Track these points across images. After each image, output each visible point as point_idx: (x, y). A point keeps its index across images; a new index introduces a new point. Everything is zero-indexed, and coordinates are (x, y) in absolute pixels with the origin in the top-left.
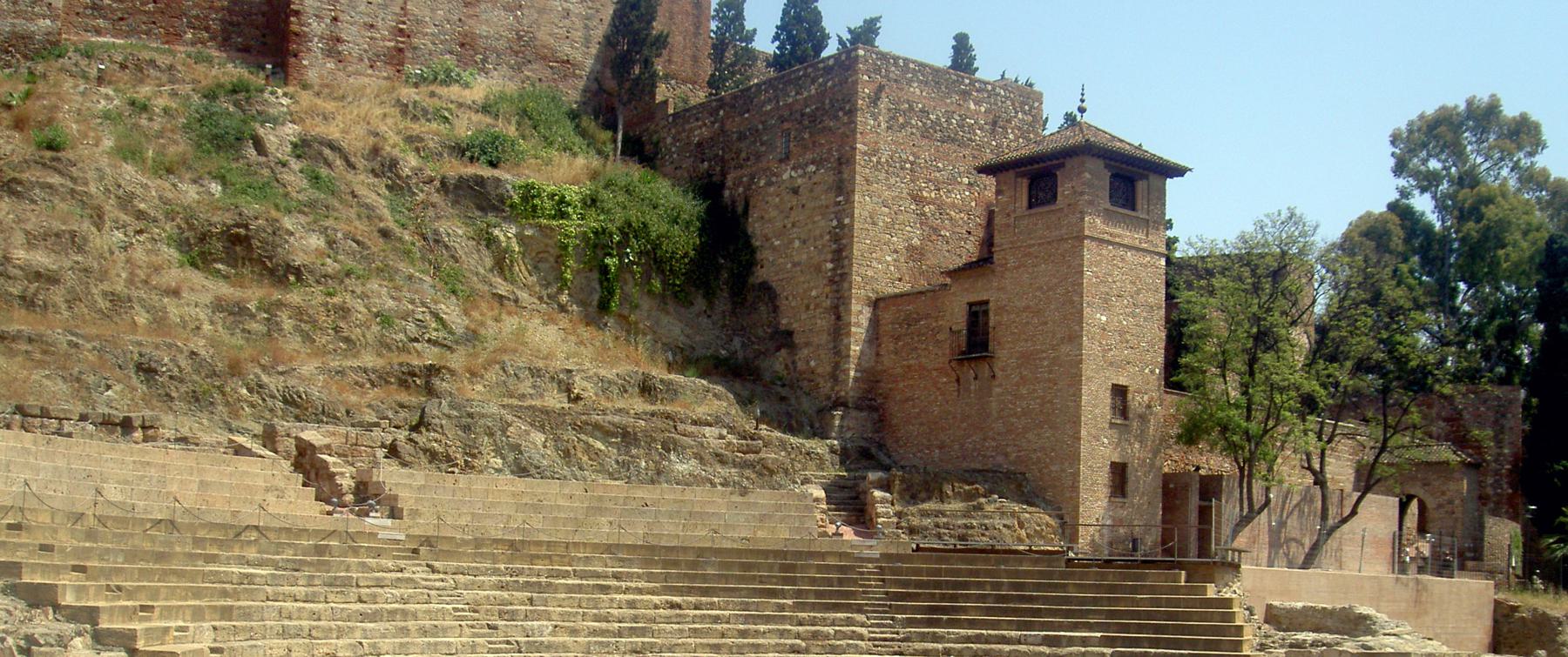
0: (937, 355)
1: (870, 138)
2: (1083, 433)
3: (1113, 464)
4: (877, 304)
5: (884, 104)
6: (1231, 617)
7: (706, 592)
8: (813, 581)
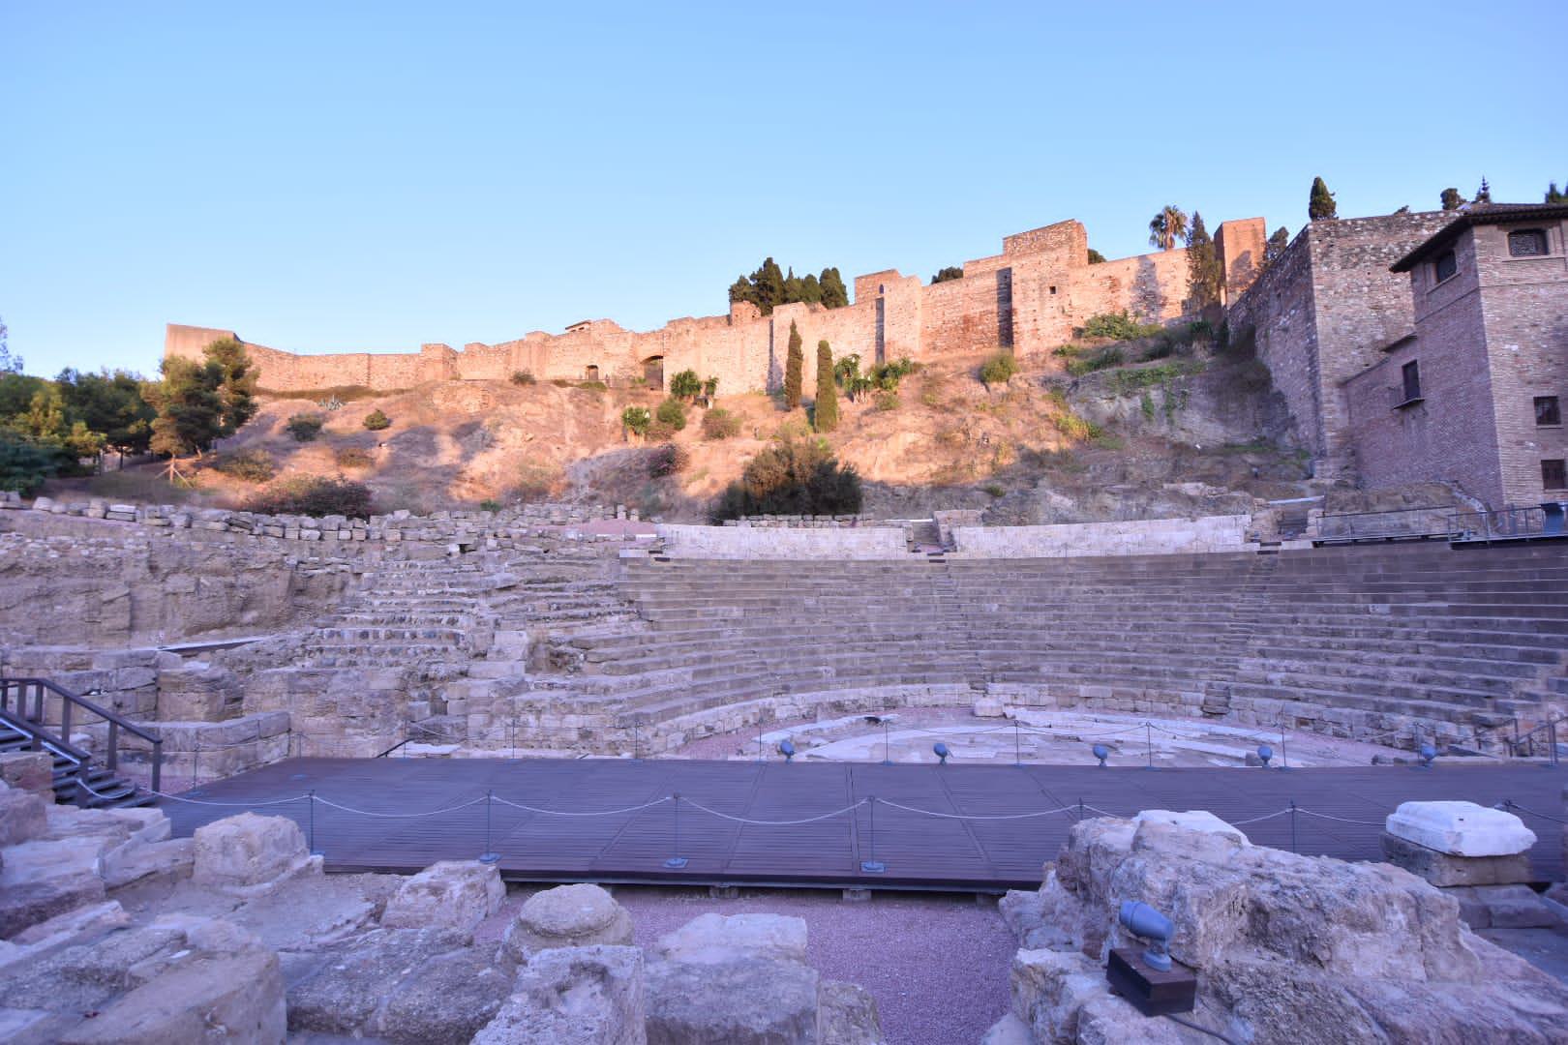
0: (1383, 409)
1: (1327, 278)
3: (1544, 462)
4: (1344, 384)
5: (1336, 253)
8: (1212, 572)
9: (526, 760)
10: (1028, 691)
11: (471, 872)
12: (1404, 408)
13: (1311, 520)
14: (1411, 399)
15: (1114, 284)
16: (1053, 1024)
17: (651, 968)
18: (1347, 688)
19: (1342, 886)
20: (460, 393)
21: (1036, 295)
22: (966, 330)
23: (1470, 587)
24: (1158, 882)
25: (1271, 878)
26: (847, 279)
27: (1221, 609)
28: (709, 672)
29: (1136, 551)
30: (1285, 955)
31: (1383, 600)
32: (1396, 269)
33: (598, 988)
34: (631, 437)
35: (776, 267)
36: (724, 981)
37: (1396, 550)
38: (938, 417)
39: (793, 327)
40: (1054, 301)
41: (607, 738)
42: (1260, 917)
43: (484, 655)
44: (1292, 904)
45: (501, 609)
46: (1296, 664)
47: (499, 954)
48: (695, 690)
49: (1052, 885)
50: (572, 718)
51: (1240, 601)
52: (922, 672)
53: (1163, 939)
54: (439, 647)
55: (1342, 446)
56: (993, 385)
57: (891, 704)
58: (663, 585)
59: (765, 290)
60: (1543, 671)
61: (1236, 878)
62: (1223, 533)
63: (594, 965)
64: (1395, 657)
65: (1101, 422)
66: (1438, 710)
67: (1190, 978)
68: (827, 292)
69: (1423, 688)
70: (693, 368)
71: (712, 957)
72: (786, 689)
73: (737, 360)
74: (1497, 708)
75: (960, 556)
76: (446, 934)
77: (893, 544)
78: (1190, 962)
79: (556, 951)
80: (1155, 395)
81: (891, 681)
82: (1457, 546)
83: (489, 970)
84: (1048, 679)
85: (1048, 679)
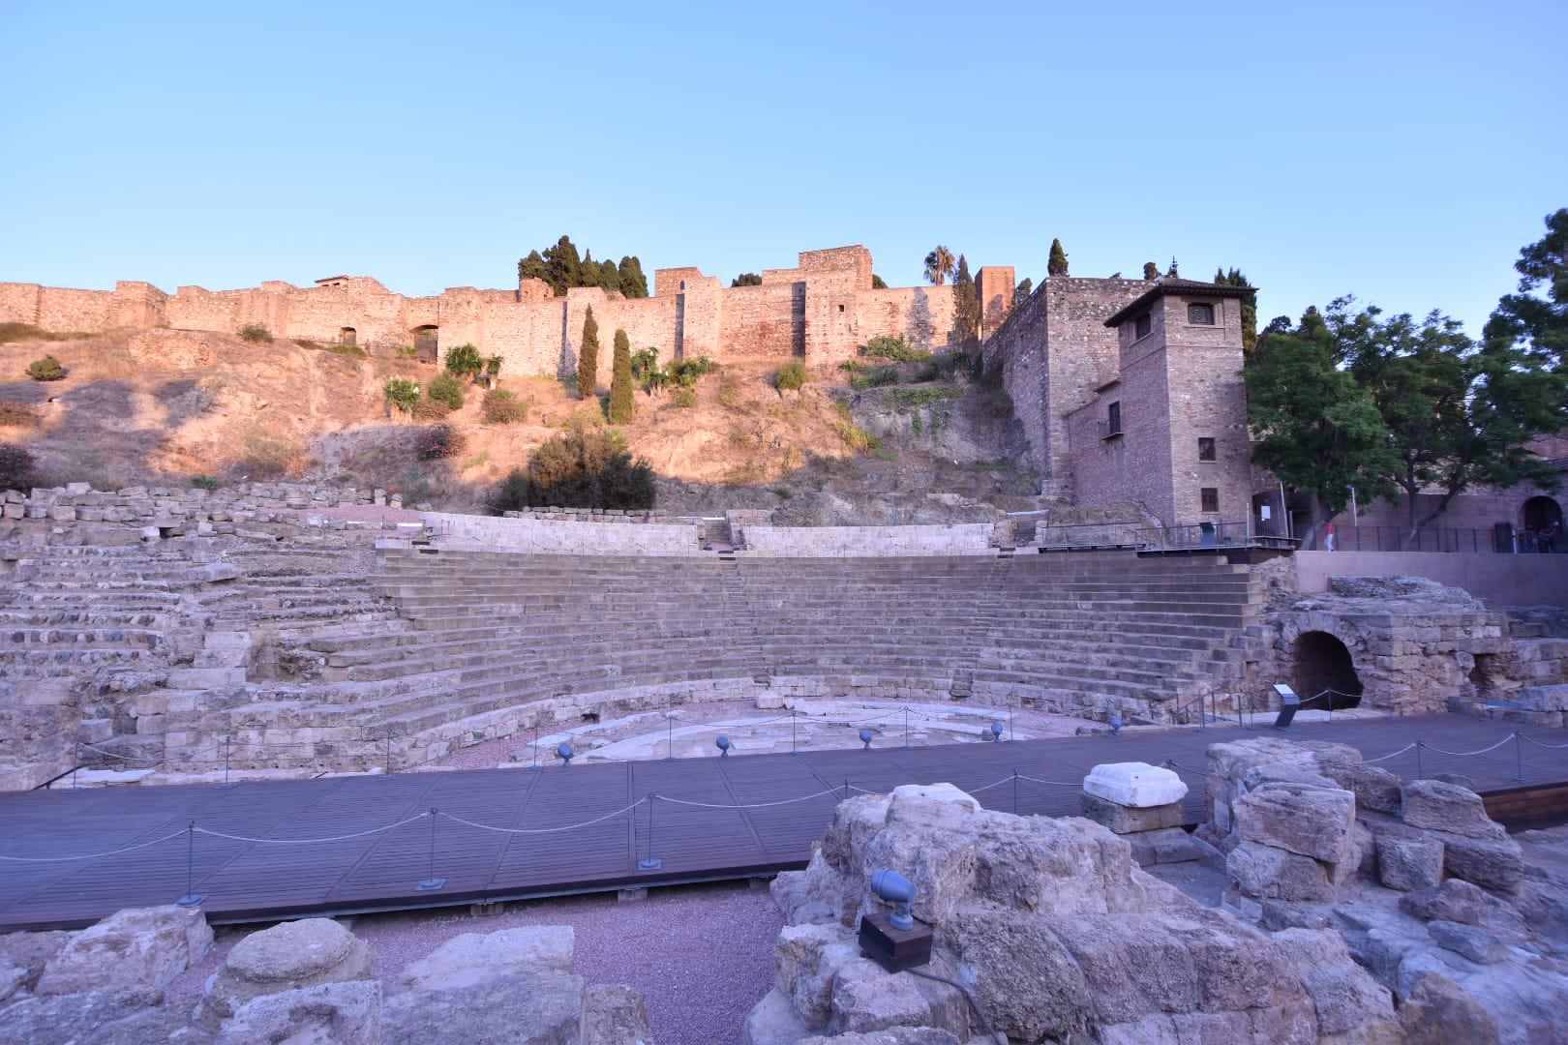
0: (1094, 439)
2: (1174, 472)
4: (1066, 417)
5: (1066, 306)
6: (1243, 588)
7: (894, 582)
9: (243, 783)
10: (806, 682)
11: (166, 919)
12: (1109, 440)
13: (1038, 530)
14: (1114, 436)
15: (894, 310)
16: (810, 993)
17: (393, 1001)
18: (1060, 672)
19: (1048, 839)
20: (168, 345)
21: (827, 311)
22: (763, 335)
23: (1150, 588)
24: (904, 850)
25: (994, 837)
26: (648, 270)
27: (968, 605)
28: (481, 675)
29: (903, 553)
30: (1003, 903)
31: (1087, 598)
32: (1109, 324)
33: (324, 1032)
34: (395, 413)
35: (573, 247)
36: (480, 1003)
37: (1098, 557)
38: (733, 418)
39: (589, 312)
40: (842, 320)
41: (352, 752)
42: (985, 872)
43: (188, 662)
44: (1010, 858)
45: (212, 607)
46: (1023, 652)
47: (199, 1009)
48: (462, 695)
49: (818, 863)
50: (307, 732)
51: (982, 597)
52: (709, 667)
53: (905, 901)
54: (126, 652)
55: (1064, 468)
56: (786, 392)
57: (676, 701)
58: (430, 580)
59: (559, 269)
60: (1197, 655)
61: (967, 839)
62: (972, 539)
63: (320, 1006)
64: (1094, 645)
65: (879, 434)
66: (1124, 689)
67: (928, 933)
68: (626, 280)
69: (1113, 670)
70: (474, 344)
71: (467, 980)
72: (568, 689)
73: (526, 339)
74: (1165, 686)
75: (750, 554)
76: (126, 995)
77: (684, 540)
78: (929, 919)
79: (272, 997)
80: (924, 414)
81: (678, 677)
82: (1140, 554)
83: (184, 1030)
84: (825, 671)
85: (825, 671)
